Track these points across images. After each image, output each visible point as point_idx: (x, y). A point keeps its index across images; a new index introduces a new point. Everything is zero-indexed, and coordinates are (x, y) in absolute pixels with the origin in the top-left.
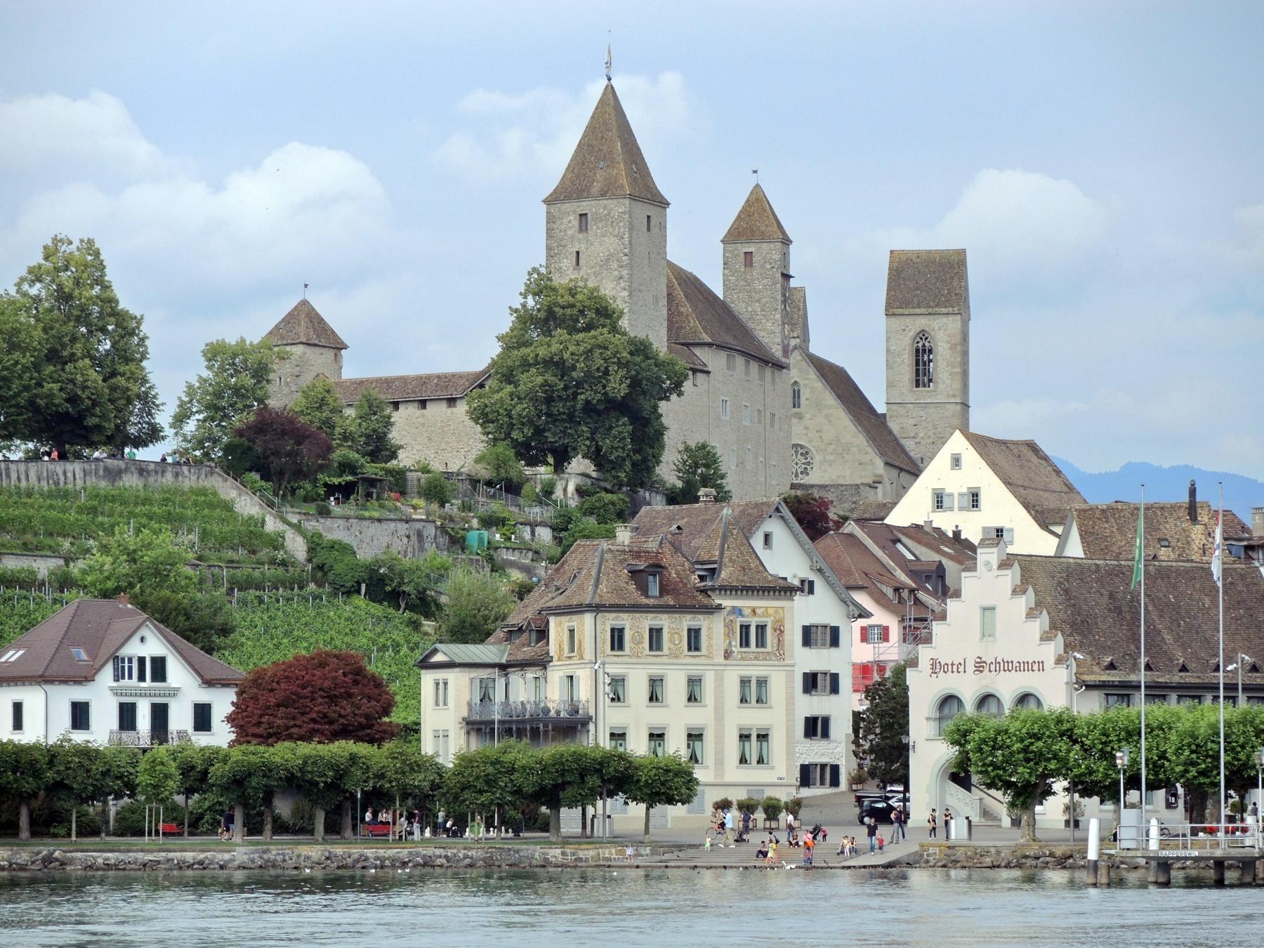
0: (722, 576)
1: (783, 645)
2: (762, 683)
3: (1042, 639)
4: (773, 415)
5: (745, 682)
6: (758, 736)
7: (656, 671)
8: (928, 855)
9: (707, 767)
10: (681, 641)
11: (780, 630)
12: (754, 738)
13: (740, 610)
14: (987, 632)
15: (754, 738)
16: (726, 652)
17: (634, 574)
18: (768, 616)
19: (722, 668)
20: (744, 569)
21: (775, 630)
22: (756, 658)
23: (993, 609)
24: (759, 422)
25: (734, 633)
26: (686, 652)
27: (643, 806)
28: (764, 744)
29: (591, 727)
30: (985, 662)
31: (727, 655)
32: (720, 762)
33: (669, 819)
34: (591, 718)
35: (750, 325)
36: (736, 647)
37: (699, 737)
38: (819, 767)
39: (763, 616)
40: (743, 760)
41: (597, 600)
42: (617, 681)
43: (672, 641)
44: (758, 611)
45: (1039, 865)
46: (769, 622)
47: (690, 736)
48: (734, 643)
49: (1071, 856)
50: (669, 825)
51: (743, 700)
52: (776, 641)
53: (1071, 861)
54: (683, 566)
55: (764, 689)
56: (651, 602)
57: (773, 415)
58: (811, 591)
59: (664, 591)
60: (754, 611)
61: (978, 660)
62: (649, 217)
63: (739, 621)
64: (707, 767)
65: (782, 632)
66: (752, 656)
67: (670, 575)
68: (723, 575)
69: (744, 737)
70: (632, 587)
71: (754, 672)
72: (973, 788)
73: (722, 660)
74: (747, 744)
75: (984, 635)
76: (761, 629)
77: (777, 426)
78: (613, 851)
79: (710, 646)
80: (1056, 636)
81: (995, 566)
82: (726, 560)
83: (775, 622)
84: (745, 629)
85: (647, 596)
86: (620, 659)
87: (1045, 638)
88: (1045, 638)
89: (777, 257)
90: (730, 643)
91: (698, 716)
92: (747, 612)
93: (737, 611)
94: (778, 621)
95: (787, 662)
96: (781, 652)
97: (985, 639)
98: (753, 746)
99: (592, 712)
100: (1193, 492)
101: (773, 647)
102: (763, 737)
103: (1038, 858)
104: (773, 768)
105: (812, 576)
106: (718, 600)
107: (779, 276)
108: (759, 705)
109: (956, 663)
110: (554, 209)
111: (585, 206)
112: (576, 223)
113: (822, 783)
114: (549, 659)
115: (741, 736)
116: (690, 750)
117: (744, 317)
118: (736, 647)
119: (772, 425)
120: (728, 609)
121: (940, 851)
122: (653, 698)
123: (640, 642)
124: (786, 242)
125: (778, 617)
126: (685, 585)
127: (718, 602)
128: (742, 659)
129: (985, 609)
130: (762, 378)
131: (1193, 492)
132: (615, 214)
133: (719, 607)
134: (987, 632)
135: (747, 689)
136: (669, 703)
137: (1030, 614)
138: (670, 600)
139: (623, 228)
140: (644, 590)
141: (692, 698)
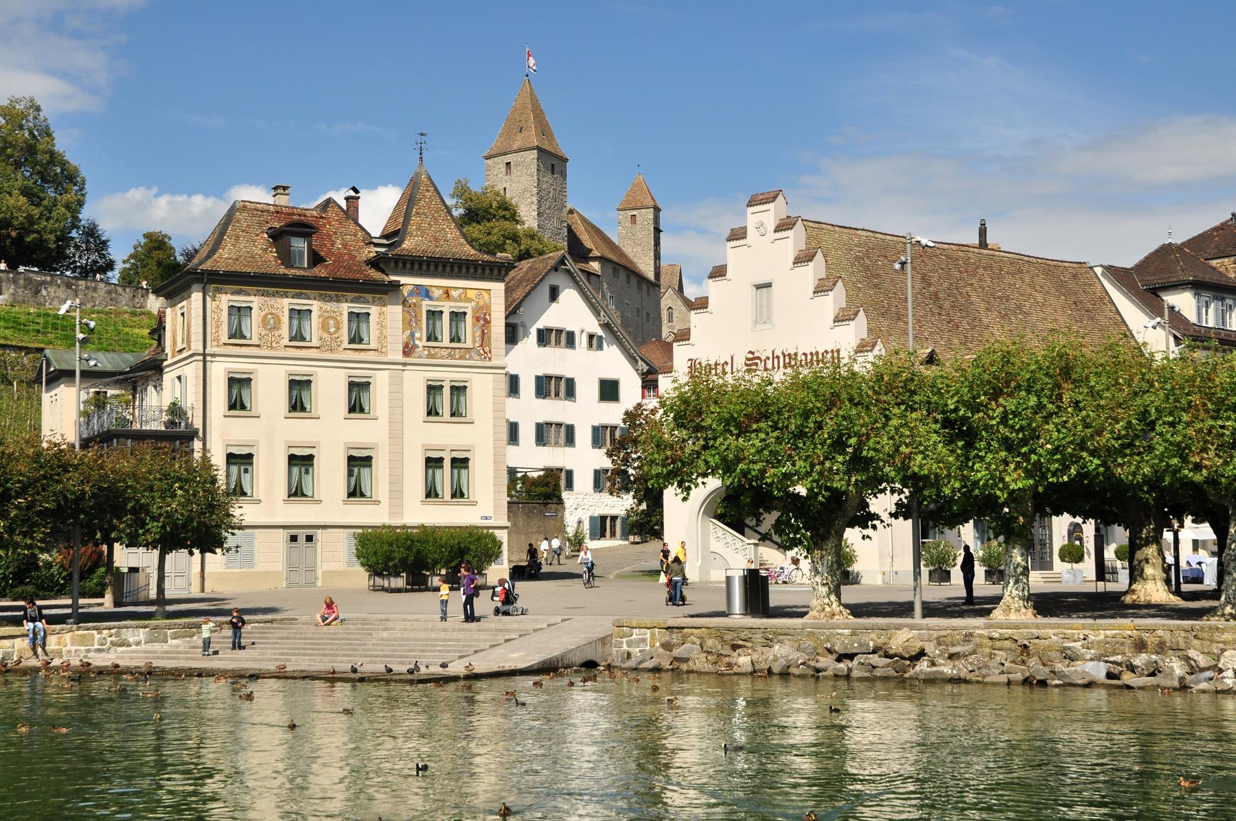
0: (404, 246)
1: (490, 338)
2: (458, 390)
3: (837, 320)
4: (648, 314)
5: (433, 390)
6: (454, 460)
7: (300, 370)
8: (629, 644)
9: (378, 502)
10: (338, 328)
11: (485, 320)
12: (447, 464)
13: (427, 291)
14: (763, 316)
15: (447, 464)
16: (406, 346)
17: (277, 237)
18: (469, 300)
19: (400, 367)
20: (436, 240)
21: (478, 319)
22: (451, 356)
23: (769, 285)
24: (638, 316)
25: (418, 321)
26: (346, 344)
27: (156, 553)
28: (464, 472)
29: (197, 444)
30: (759, 358)
31: (408, 350)
32: (397, 495)
33: (319, 574)
34: (196, 433)
35: (635, 260)
36: (421, 342)
37: (367, 461)
38: (608, 521)
39: (460, 301)
40: (431, 493)
41: (207, 266)
42: (239, 381)
43: (325, 327)
44: (454, 293)
45: (856, 674)
46: (469, 308)
47: (351, 459)
48: (417, 335)
49: (922, 654)
50: (319, 583)
51: (432, 412)
52: (478, 333)
53: (923, 666)
54: (355, 235)
55: (462, 399)
56: (292, 272)
57: (648, 314)
58: (600, 347)
59: (316, 259)
60: (447, 293)
61: (750, 356)
62: (553, 165)
63: (426, 305)
64: (378, 502)
65: (488, 322)
66: (445, 353)
67: (333, 245)
68: (407, 244)
69: (433, 463)
70: (272, 254)
71: (447, 376)
72: (747, 530)
73: (399, 357)
74: (438, 472)
75: (756, 322)
76: (457, 316)
77: (651, 322)
78: (67, 637)
79: (382, 337)
80: (856, 314)
81: (771, 227)
82: (412, 228)
83: (477, 310)
84: (434, 315)
85: (289, 265)
86: (244, 351)
87: (841, 318)
88: (841, 318)
89: (651, 217)
90: (412, 335)
91: (361, 433)
92: (437, 293)
93: (426, 293)
94: (481, 308)
95: (494, 363)
96: (487, 349)
97: (758, 327)
98: (444, 477)
99: (198, 424)
100: (983, 232)
101: (474, 342)
102: (460, 463)
103: (851, 657)
104: (475, 503)
105: (600, 332)
106: (393, 278)
107: (652, 229)
108: (454, 419)
109: (722, 362)
110: (488, 161)
111: (507, 158)
112: (504, 170)
113: (613, 534)
114: (164, 357)
115: (429, 461)
116: (353, 480)
117: (631, 256)
118: (420, 339)
119: (648, 320)
120: (410, 288)
121: (653, 635)
122: (297, 406)
123: (277, 326)
124: (657, 210)
125: (481, 303)
126: (352, 257)
127: (393, 278)
128: (430, 356)
129: (759, 287)
130: (639, 288)
131: (983, 232)
132: (528, 160)
133: (396, 286)
134: (763, 316)
135: (438, 398)
136: (320, 413)
137: (821, 289)
138: (321, 272)
139: (533, 169)
140: (286, 257)
141: (356, 407)
